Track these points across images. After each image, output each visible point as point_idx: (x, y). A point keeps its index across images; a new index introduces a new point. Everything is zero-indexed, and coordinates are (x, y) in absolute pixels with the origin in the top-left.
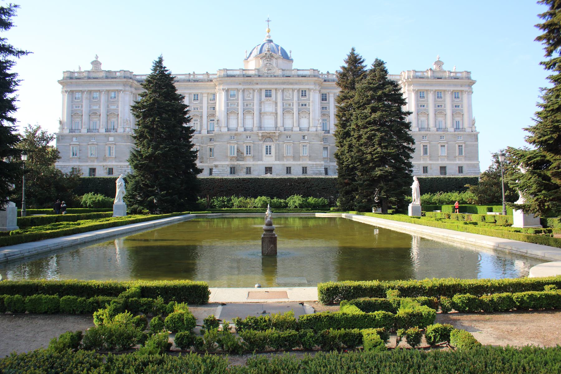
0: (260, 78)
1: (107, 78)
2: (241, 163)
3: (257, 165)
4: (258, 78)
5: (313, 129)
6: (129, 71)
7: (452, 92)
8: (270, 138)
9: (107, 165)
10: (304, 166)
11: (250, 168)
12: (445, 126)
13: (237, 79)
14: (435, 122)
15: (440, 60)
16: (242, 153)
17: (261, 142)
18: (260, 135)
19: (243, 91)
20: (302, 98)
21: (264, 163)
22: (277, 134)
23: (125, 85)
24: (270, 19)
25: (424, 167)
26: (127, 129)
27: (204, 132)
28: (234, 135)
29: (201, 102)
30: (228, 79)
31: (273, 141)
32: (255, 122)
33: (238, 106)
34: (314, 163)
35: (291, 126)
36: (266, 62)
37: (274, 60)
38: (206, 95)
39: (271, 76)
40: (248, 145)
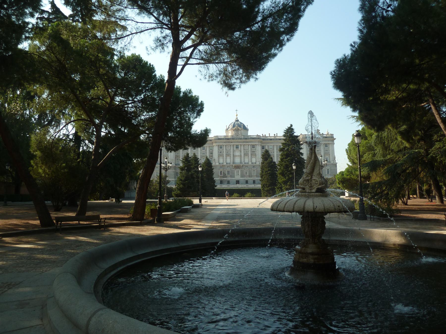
2: (225, 179)
3: (232, 179)
4: (232, 140)
5: (258, 163)
11: (229, 181)
13: (223, 140)
16: (225, 174)
17: (234, 169)
18: (234, 166)
19: (226, 146)
21: (235, 179)
22: (241, 166)
28: (222, 166)
29: (206, 151)
30: (219, 140)
35: (247, 162)
36: (236, 132)
37: (240, 131)
39: (238, 139)
40: (228, 170)
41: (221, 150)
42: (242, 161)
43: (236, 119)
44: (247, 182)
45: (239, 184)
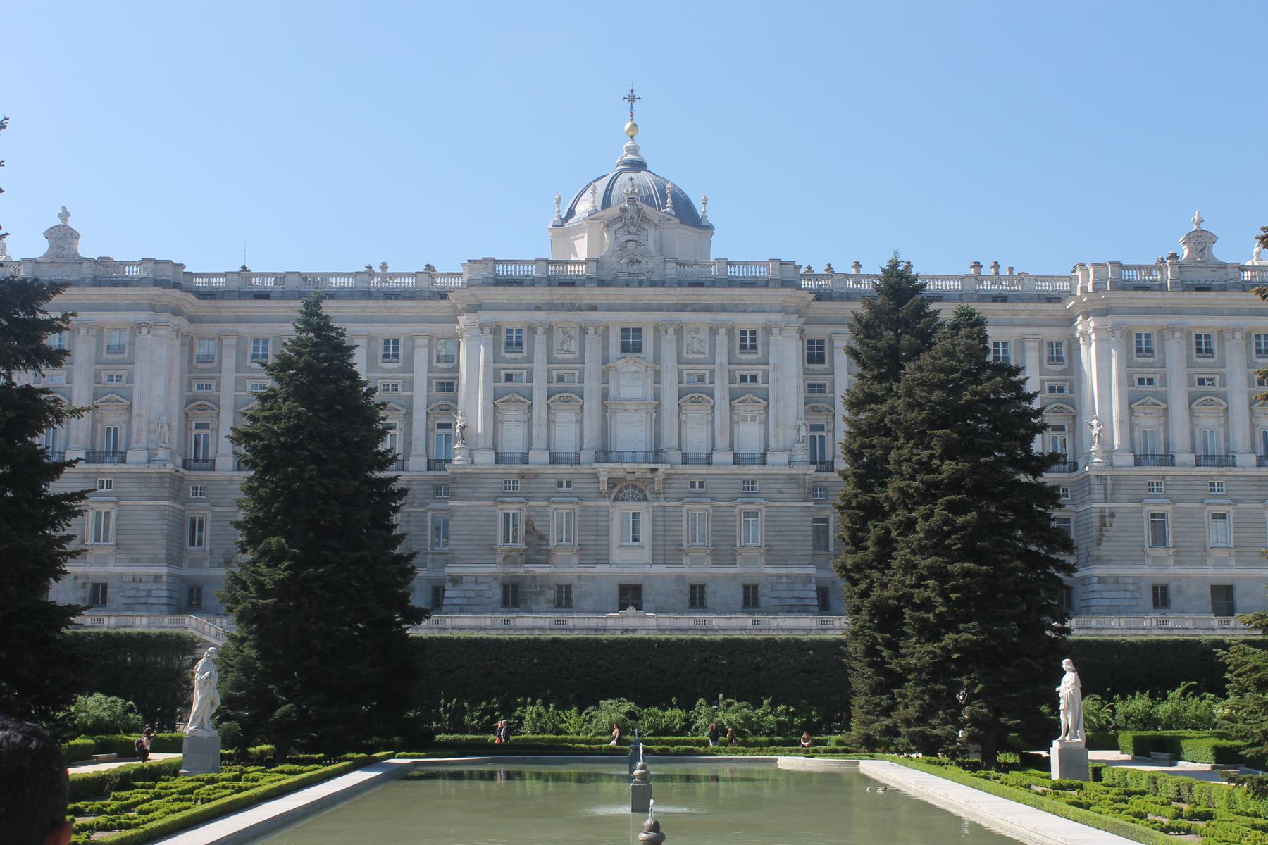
0: (606, 290)
1: (97, 282)
2: (539, 570)
3: (593, 578)
4: (598, 290)
6: (170, 262)
7: (1248, 335)
8: (635, 487)
9: (87, 576)
10: (748, 582)
11: (569, 587)
12: (1227, 449)
14: (1192, 435)
15: (1203, 227)
16: (542, 538)
18: (604, 478)
19: (549, 331)
20: (743, 357)
22: (661, 473)
23: (153, 309)
24: (637, 93)
25: (1155, 588)
26: (162, 454)
27: (417, 464)
29: (409, 368)
30: (500, 290)
31: (645, 499)
32: (586, 434)
33: (530, 380)
34: (784, 571)
35: (704, 449)
36: (623, 239)
37: (652, 232)
38: (425, 342)
39: (641, 284)
41: (515, 361)
42: (665, 444)
43: (630, 157)
44: (697, 597)
45: (638, 607)
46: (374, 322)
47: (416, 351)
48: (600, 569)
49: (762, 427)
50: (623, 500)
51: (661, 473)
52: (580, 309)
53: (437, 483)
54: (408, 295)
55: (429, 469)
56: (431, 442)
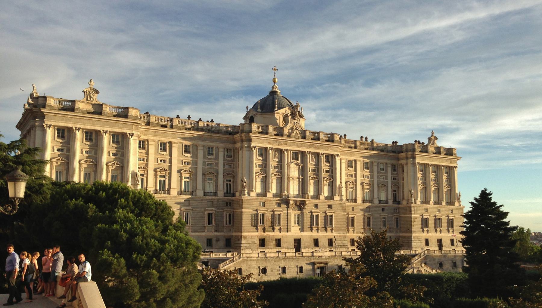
2: (271, 234)
3: (287, 236)
29: (217, 158)
34: (339, 234)
38: (222, 150)
46: (205, 140)
47: (220, 153)
48: (289, 233)
49: (331, 187)
50: (294, 210)
51: (307, 203)
52: (282, 144)
53: (227, 201)
54: (216, 132)
55: (224, 196)
56: (224, 186)
